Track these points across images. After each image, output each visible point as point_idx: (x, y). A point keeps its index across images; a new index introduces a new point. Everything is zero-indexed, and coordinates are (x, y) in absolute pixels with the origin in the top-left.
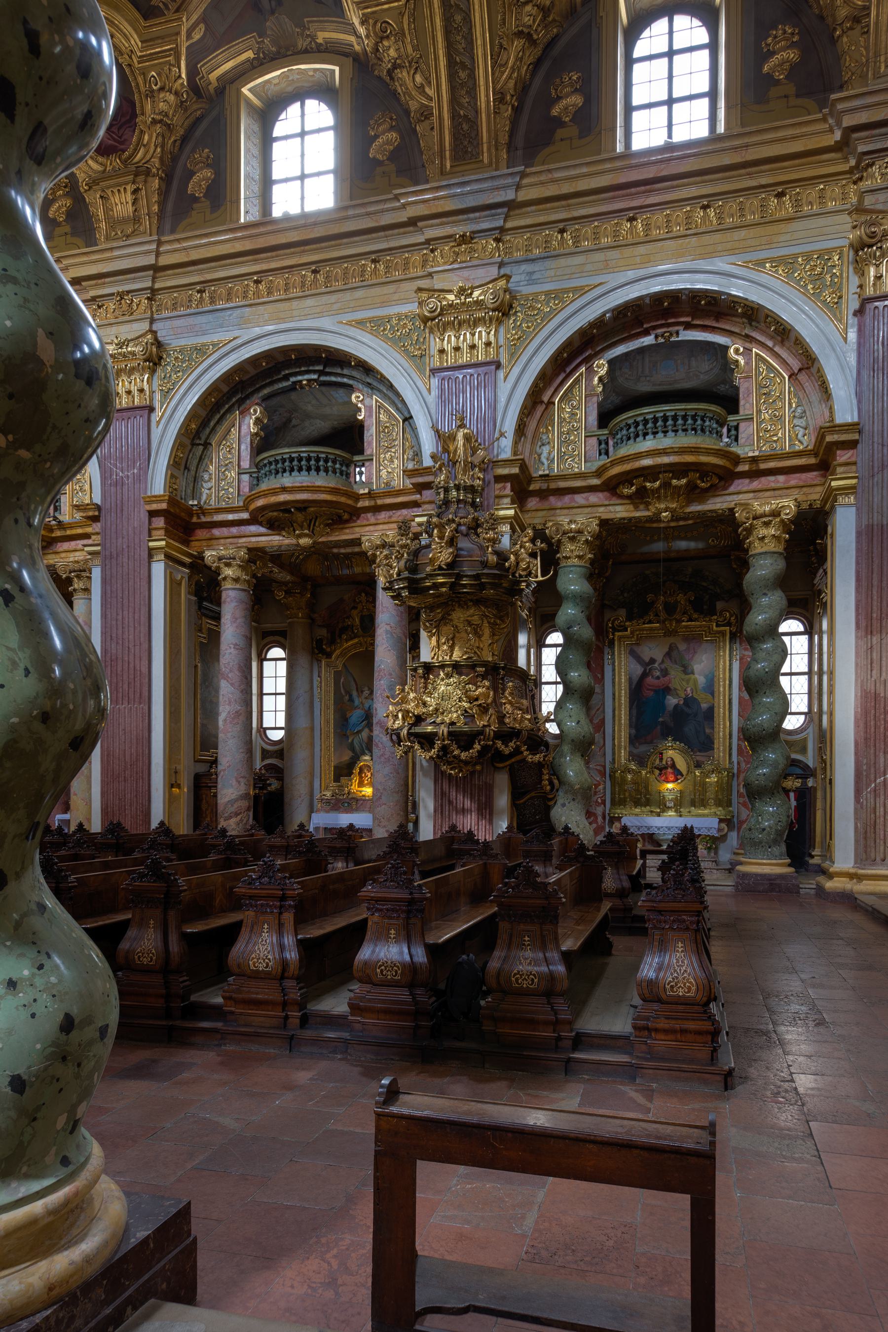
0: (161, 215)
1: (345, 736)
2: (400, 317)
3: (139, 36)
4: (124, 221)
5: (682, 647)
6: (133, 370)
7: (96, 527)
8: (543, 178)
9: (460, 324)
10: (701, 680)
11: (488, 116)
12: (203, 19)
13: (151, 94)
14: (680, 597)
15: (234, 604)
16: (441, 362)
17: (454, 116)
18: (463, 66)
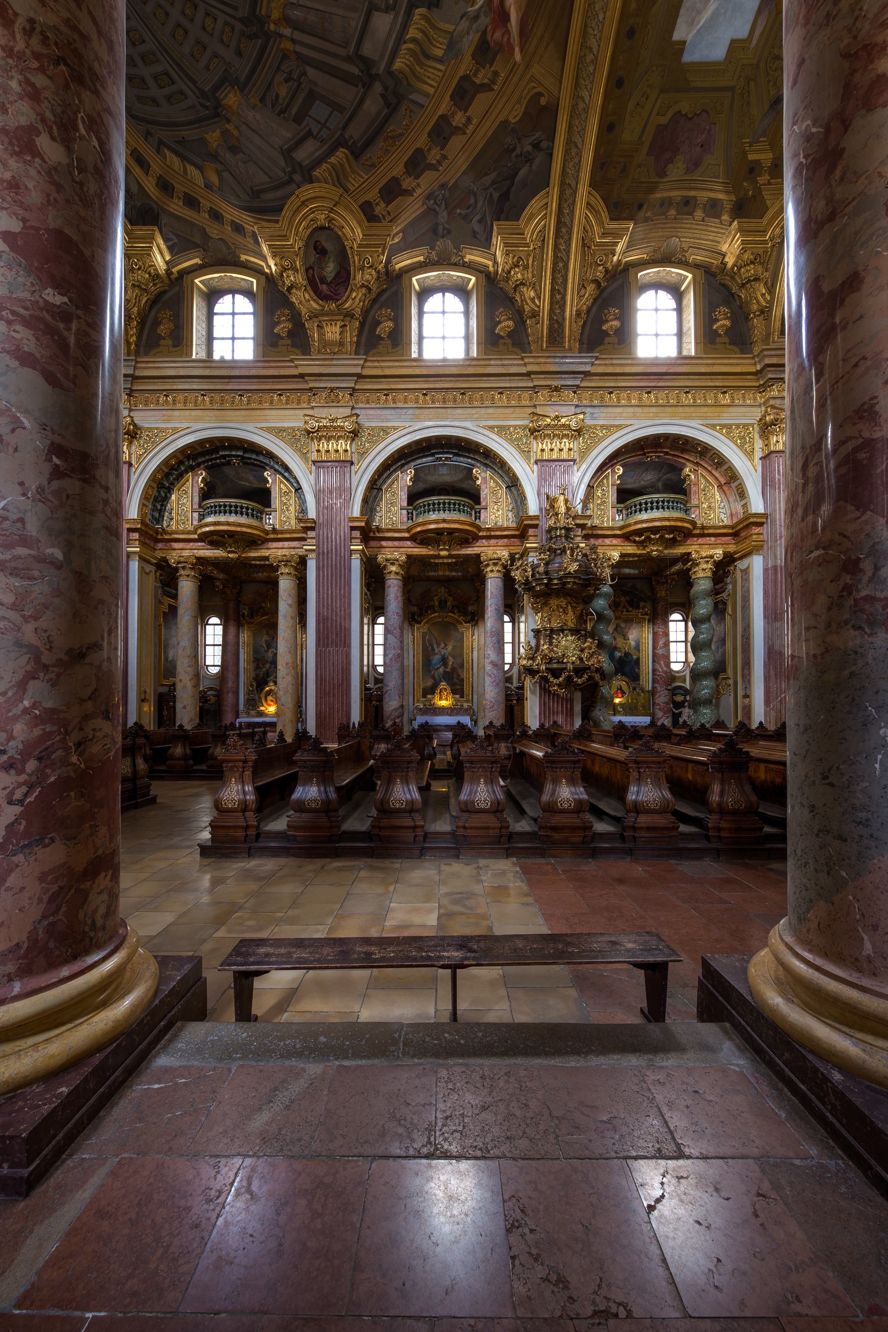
0: (358, 343)
1: (430, 671)
2: (515, 427)
3: (362, 231)
4: (332, 343)
5: (623, 625)
6: (340, 437)
7: (311, 534)
8: (607, 362)
9: (554, 436)
10: (633, 643)
11: (570, 323)
12: (403, 231)
13: (362, 268)
14: (623, 599)
15: (396, 588)
16: (542, 455)
17: (550, 319)
18: (559, 292)
